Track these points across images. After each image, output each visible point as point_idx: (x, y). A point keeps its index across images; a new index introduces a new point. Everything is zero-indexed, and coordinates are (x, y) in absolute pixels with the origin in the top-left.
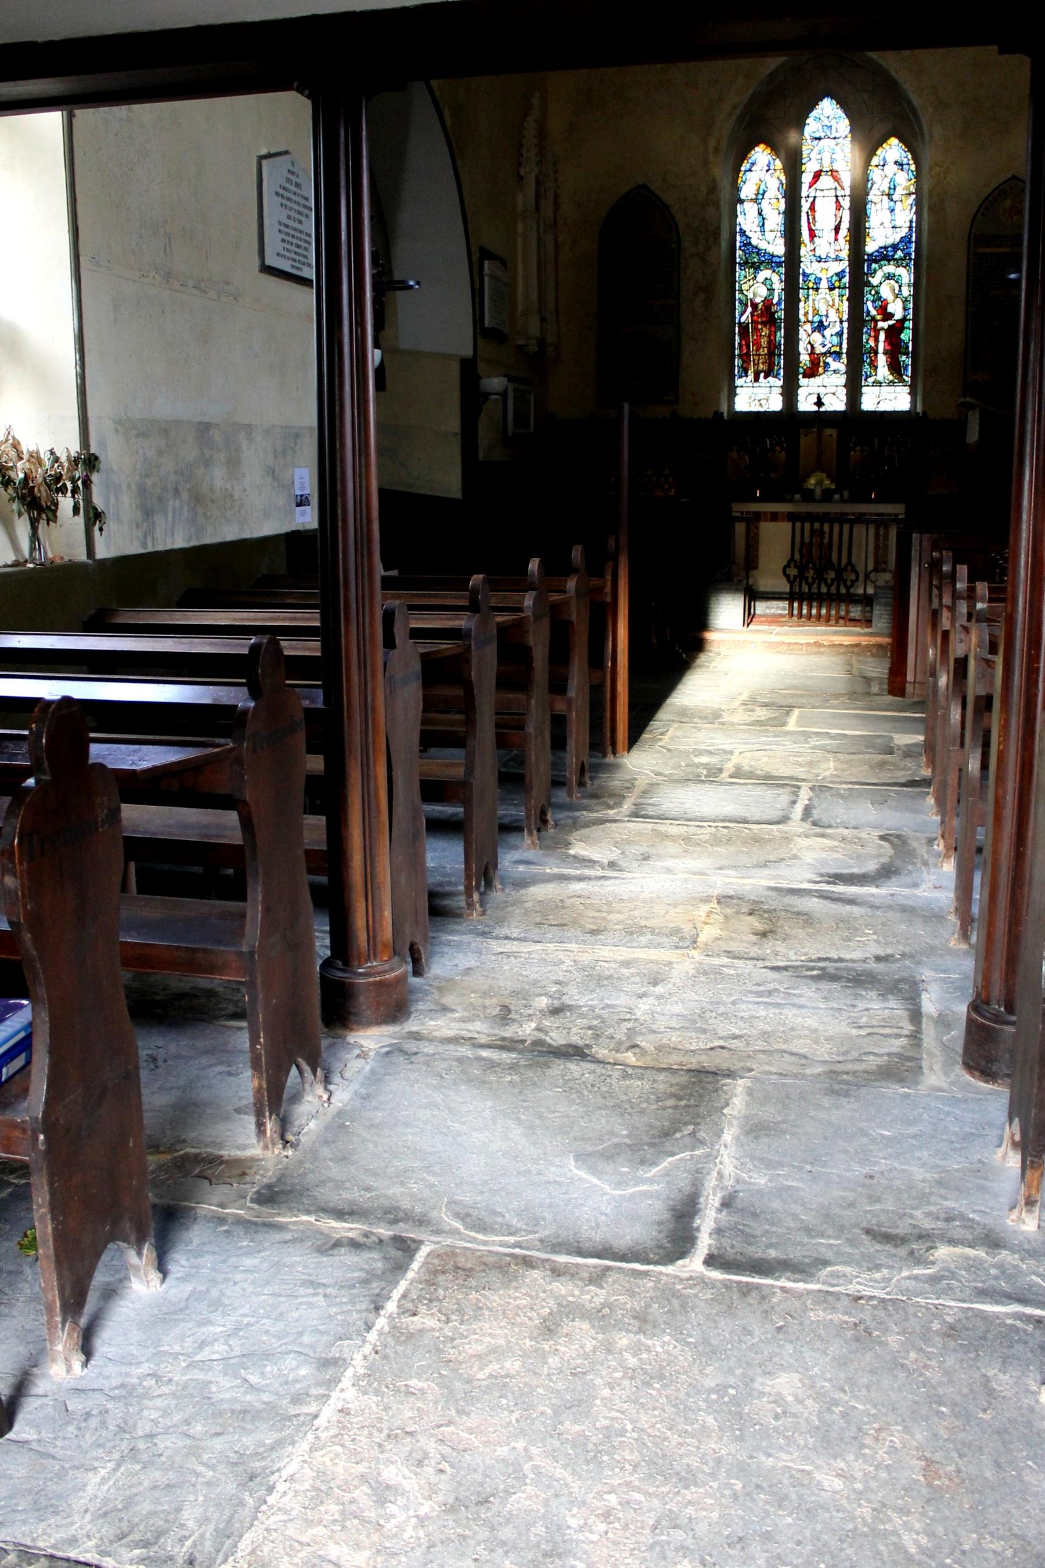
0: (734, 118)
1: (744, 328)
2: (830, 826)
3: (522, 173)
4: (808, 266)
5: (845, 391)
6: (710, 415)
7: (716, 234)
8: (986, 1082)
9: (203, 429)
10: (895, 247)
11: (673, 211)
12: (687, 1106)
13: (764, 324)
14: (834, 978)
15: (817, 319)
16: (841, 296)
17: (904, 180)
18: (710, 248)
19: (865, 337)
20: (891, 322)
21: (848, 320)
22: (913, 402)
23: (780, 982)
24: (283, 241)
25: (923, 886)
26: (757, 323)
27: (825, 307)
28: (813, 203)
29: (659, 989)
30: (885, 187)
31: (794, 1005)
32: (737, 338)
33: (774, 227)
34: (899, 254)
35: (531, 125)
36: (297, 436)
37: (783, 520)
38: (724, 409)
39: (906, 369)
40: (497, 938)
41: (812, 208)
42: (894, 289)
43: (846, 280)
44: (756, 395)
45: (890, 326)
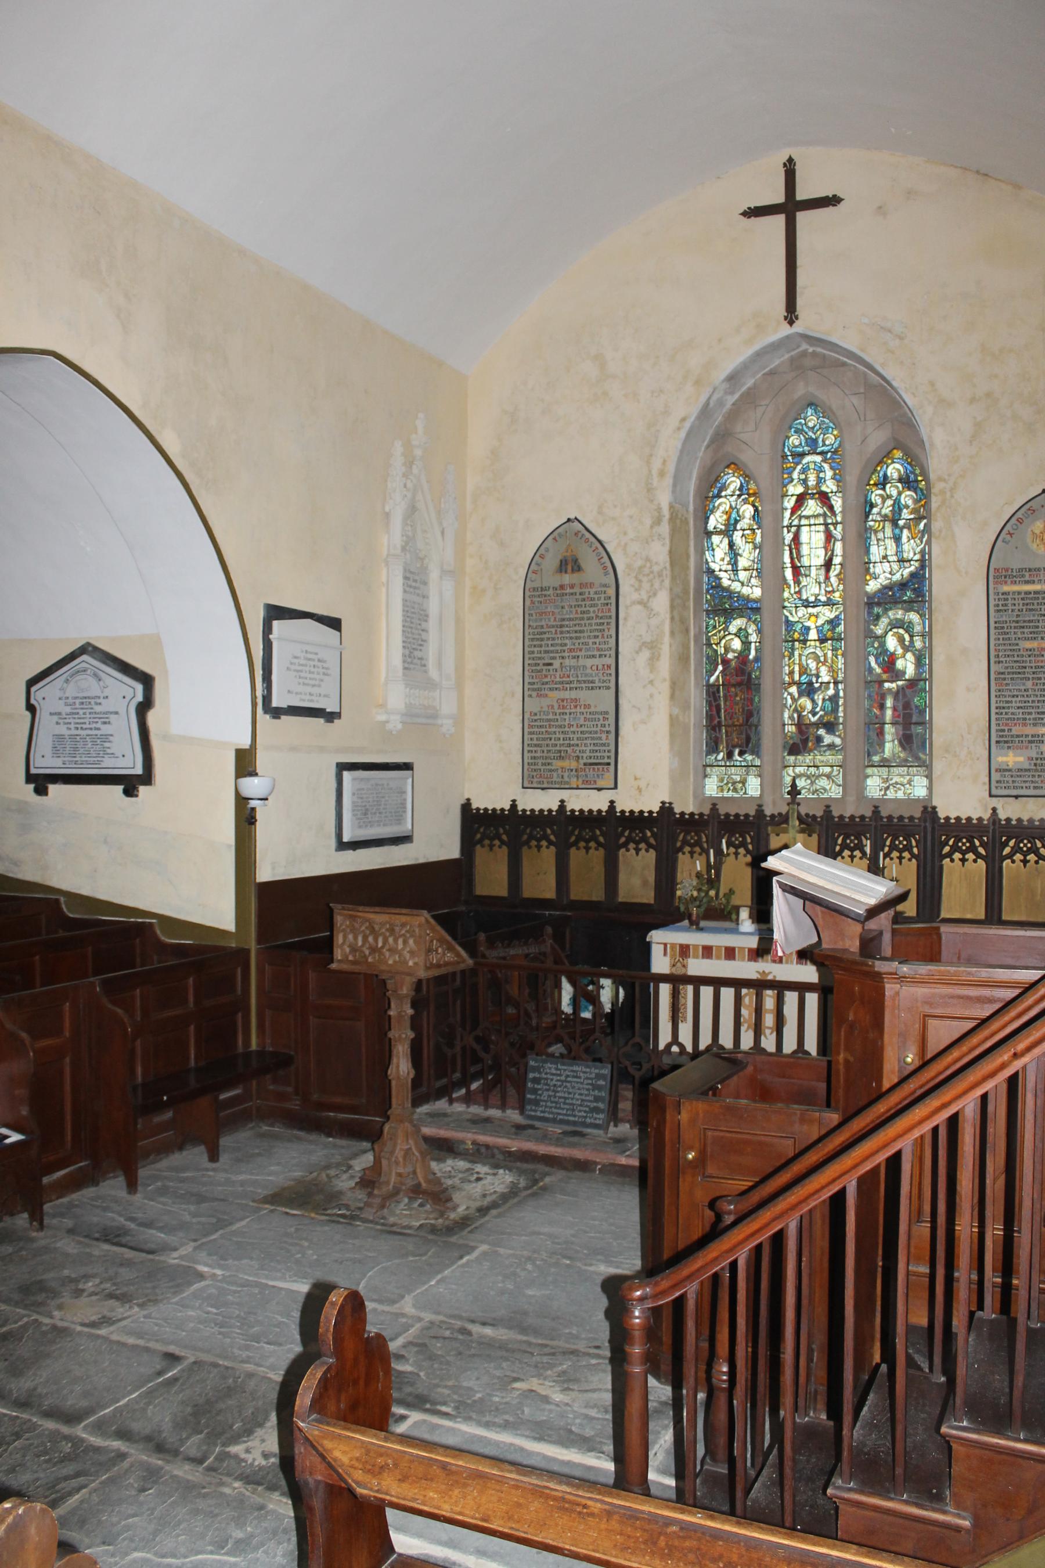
0: (683, 434)
10: (903, 585)
18: (655, 594)
20: (900, 683)
30: (887, 510)
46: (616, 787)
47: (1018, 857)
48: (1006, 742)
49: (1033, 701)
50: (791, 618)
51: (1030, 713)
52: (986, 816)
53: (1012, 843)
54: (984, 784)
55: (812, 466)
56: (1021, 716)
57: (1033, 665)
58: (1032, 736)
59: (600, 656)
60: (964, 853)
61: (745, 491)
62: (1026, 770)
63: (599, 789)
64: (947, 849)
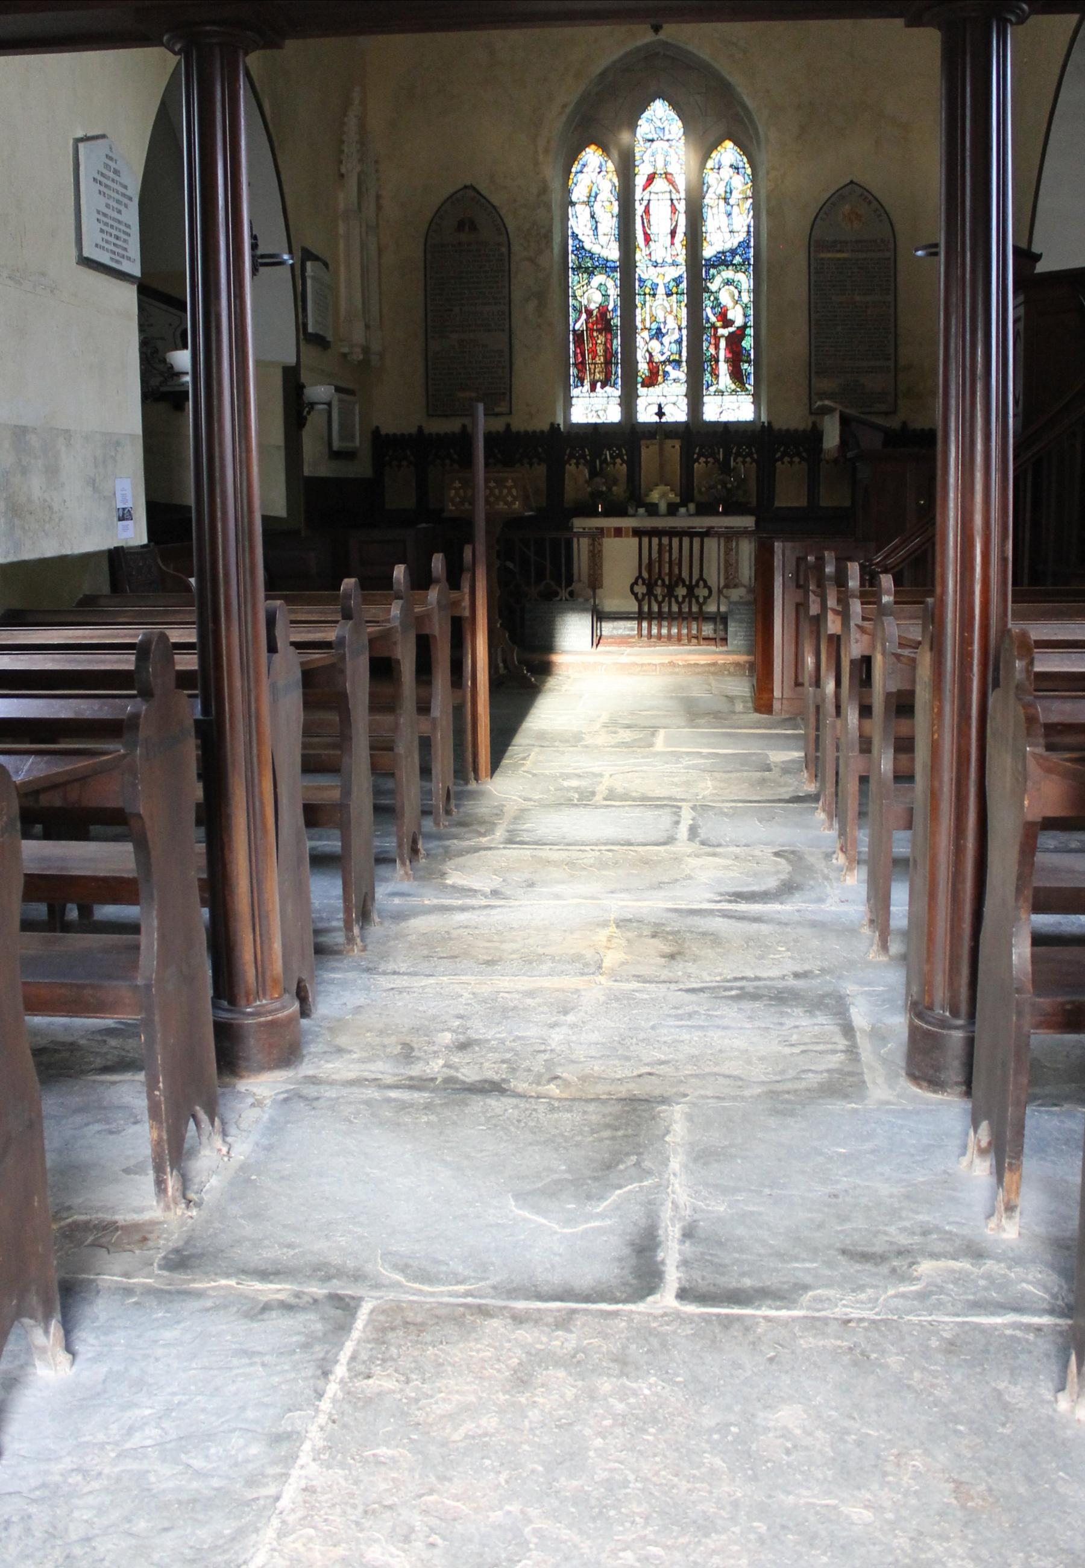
0: (564, 118)
1: (579, 337)
2: (719, 845)
3: (343, 170)
4: (643, 270)
5: (686, 400)
6: (546, 427)
7: (548, 237)
8: (935, 1092)
9: (20, 433)
10: (733, 252)
11: (503, 212)
12: (625, 1136)
13: (600, 331)
14: (755, 997)
15: (654, 326)
16: (679, 302)
17: (740, 184)
19: (705, 344)
20: (731, 329)
21: (687, 327)
22: (757, 411)
23: (699, 1005)
24: (102, 231)
25: (829, 901)
26: (592, 330)
27: (663, 314)
28: (647, 207)
29: (570, 1018)
30: (721, 191)
31: (718, 1027)
32: (572, 346)
33: (607, 230)
34: (738, 259)
35: (352, 122)
36: (118, 443)
37: (627, 536)
38: (560, 420)
39: (748, 377)
40: (384, 973)
41: (647, 211)
42: (733, 295)
43: (684, 286)
44: (593, 406)
45: (731, 334)
46: (510, 413)
50: (644, 277)
55: (660, 151)
59: (495, 304)
60: (791, 457)
61: (604, 169)
63: (497, 415)
64: (778, 455)
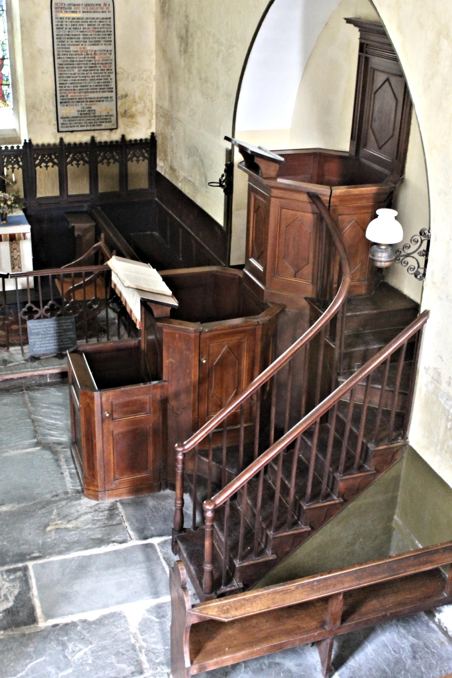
47: (74, 162)
48: (65, 102)
49: (78, 80)
51: (77, 87)
52: (58, 141)
53: (71, 156)
54: (54, 125)
56: (72, 88)
57: (78, 60)
58: (79, 99)
62: (76, 117)
64: (37, 162)
